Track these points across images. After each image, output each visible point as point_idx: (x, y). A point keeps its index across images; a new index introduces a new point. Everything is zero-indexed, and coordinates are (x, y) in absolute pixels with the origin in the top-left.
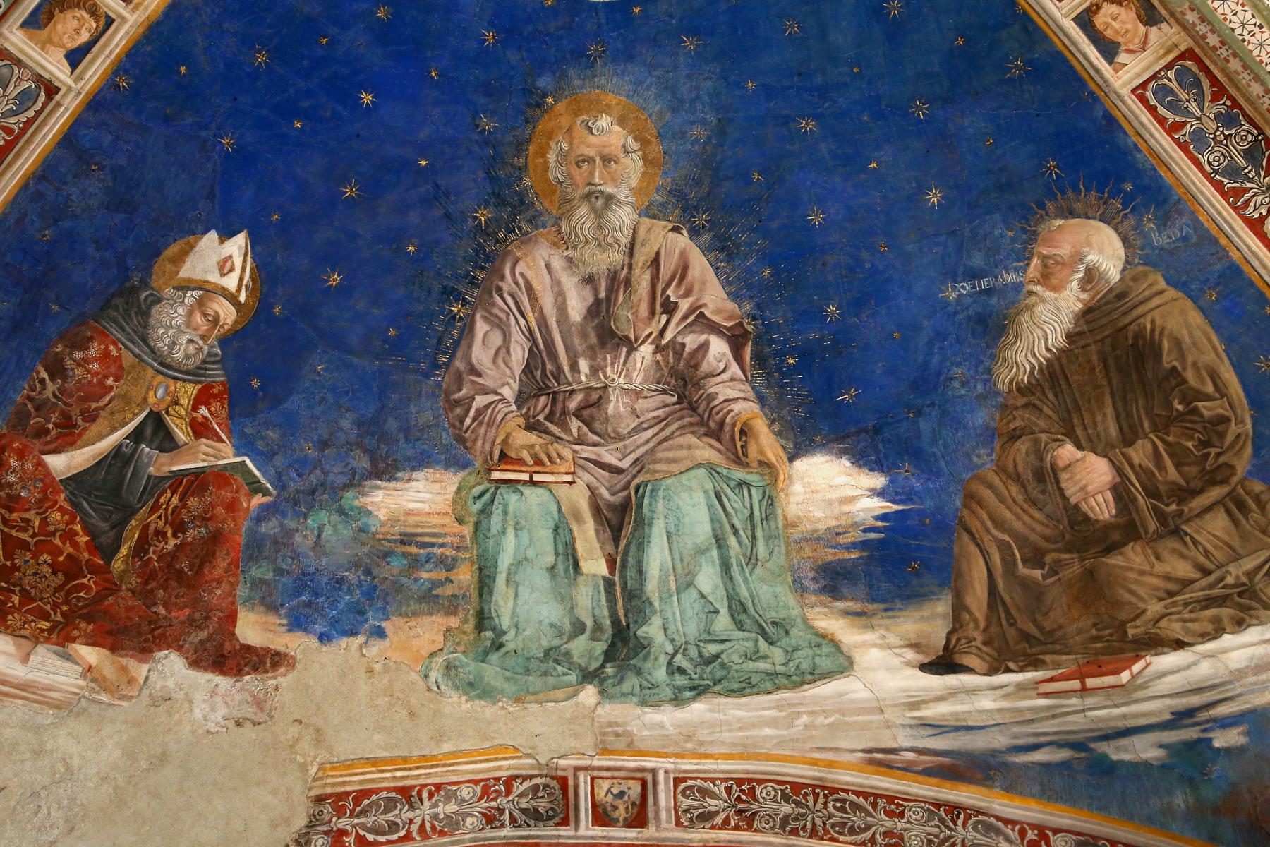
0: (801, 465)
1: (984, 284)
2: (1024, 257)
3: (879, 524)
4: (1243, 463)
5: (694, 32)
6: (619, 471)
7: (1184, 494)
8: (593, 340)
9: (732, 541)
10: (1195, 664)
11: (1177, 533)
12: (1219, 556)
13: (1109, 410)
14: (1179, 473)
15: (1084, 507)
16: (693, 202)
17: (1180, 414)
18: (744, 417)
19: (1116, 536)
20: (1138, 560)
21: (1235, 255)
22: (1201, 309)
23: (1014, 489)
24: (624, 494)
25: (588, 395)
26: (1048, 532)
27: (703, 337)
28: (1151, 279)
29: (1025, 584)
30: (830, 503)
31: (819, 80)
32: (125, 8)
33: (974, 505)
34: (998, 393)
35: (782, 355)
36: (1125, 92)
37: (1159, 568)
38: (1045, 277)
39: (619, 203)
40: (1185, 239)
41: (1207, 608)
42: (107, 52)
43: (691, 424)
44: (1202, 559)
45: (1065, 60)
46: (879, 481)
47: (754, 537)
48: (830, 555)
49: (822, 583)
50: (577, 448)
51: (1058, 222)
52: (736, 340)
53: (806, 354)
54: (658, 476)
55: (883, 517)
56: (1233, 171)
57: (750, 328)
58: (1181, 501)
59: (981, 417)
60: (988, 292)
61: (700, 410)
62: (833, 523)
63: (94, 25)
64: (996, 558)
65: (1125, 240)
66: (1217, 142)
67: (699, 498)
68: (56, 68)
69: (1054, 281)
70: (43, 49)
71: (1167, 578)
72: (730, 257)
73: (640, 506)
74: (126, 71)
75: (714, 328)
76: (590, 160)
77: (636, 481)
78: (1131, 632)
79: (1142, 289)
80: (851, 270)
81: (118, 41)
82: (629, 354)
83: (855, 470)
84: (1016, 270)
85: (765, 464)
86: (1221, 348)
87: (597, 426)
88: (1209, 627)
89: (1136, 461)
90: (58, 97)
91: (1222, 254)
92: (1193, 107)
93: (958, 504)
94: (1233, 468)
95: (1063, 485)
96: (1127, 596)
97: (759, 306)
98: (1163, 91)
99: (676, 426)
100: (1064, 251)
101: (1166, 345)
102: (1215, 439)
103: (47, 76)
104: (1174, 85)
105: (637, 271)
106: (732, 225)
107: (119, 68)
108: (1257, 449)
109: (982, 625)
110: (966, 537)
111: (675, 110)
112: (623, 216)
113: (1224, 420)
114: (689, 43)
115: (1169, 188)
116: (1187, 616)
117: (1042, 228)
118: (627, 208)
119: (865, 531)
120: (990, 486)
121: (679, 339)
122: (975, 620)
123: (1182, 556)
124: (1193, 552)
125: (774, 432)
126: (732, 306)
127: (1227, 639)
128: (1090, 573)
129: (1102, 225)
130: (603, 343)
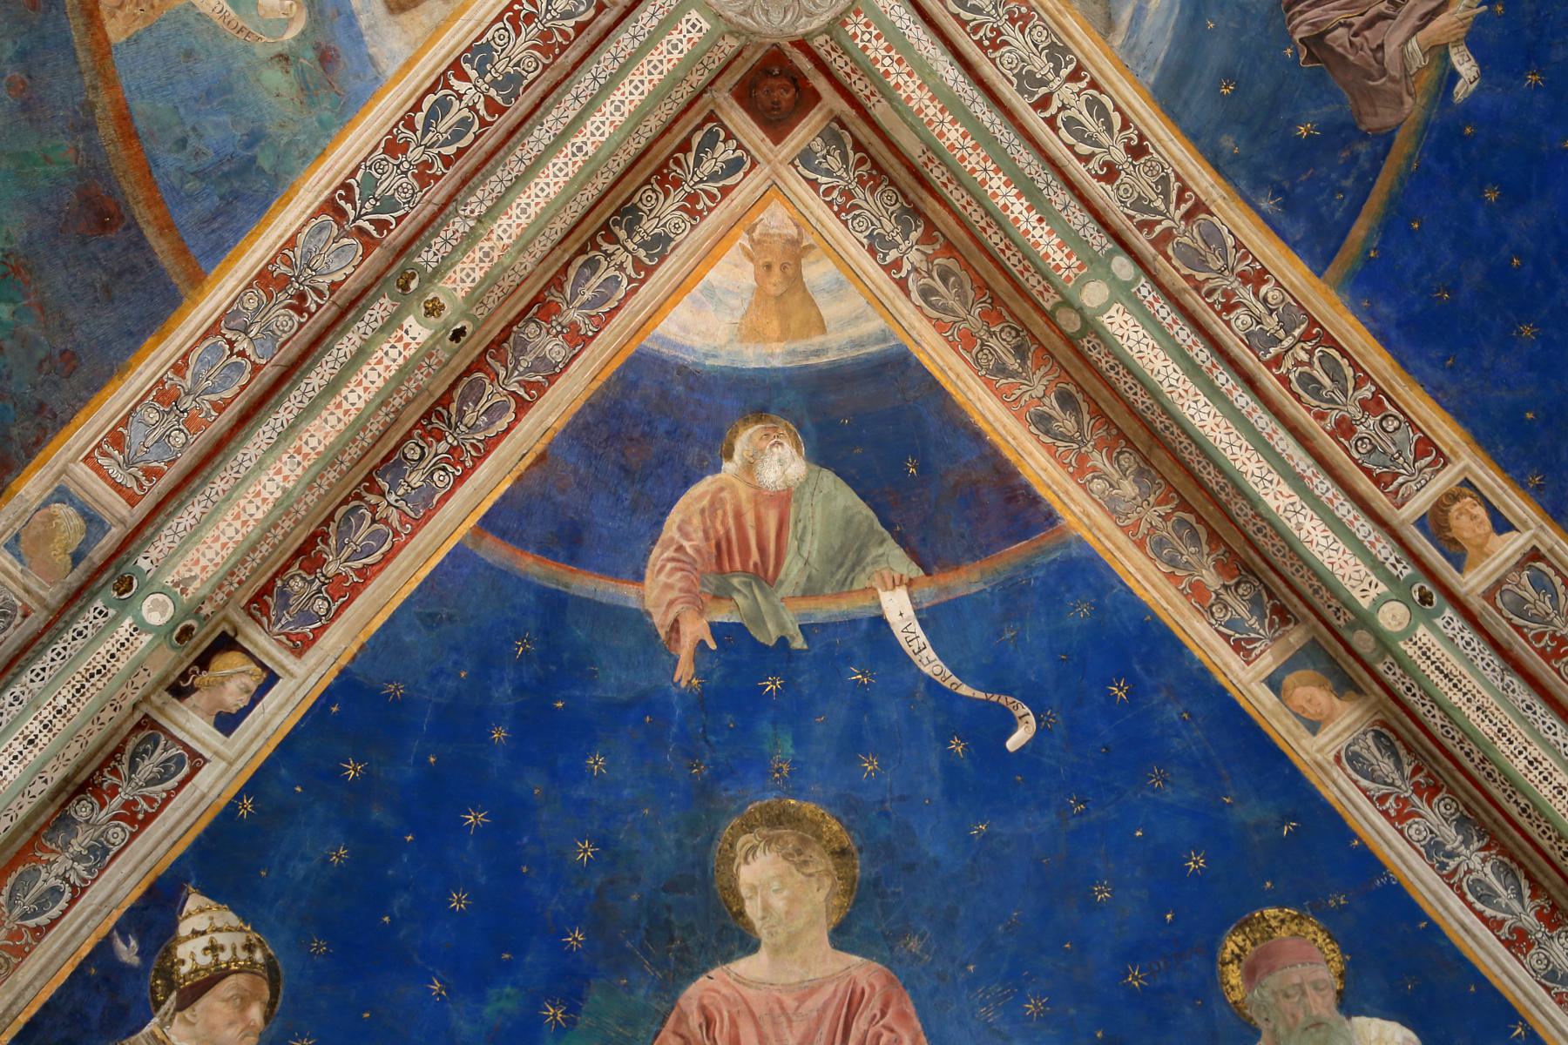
32: (1454, 465)
42: (1500, 491)
63: (1469, 499)
68: (1510, 547)
70: (1488, 556)
74: (1523, 475)
81: (1489, 478)
90: (1543, 550)
103: (1518, 557)
107: (1520, 483)
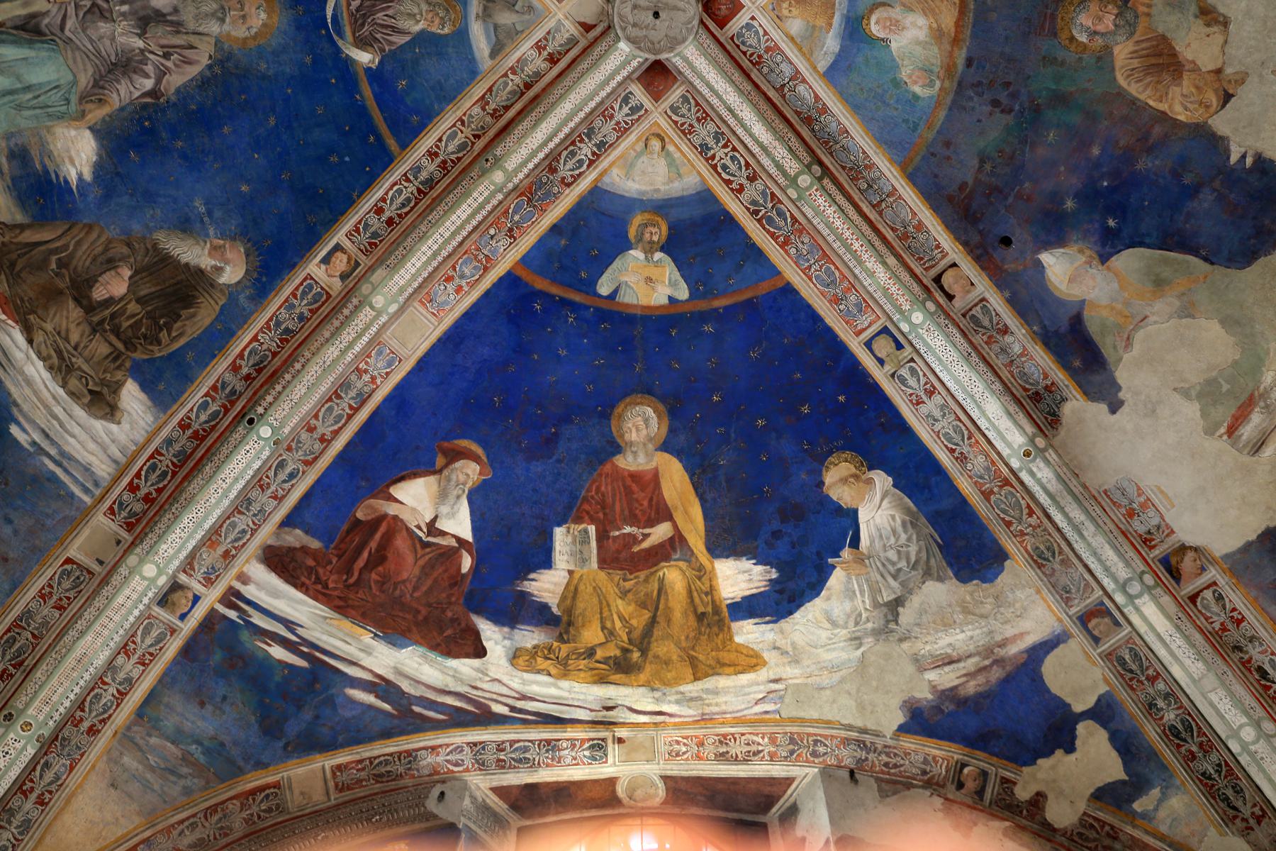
0: (88, 134)
1: (206, 219)
2: (223, 236)
3: (62, 179)
4: (138, 356)
5: (314, 62)
6: (62, 28)
7: (116, 332)
8: (142, 13)
9: (29, 96)
10: (20, 350)
11: (94, 331)
12: (86, 353)
13: (153, 289)
14: (127, 328)
15: (97, 285)
16: (226, 65)
17: (158, 322)
18: (109, 100)
19: (85, 302)
20: (75, 315)
21: (240, 333)
22: (212, 324)
23: (100, 249)
24: (47, 32)
25: (107, 11)
26: (79, 269)
27: (152, 75)
28: (223, 298)
29: (46, 261)
30: (68, 151)
31: (295, 125)
33: (86, 230)
34: (151, 234)
35: (149, 119)
36: (308, 271)
37: (72, 326)
38: (215, 248)
39: (221, 25)
40: (244, 309)
41: (55, 351)
43: (100, 71)
44: (82, 345)
45: (318, 241)
46: (88, 176)
47: (35, 108)
48: (34, 152)
49: (16, 149)
50: (73, 4)
51: (242, 250)
52: (154, 93)
53: (151, 132)
54: (63, 52)
55: (66, 181)
56: (278, 324)
57: (162, 100)
58: (112, 331)
59: (136, 227)
60: (202, 221)
61: (109, 75)
62: (56, 154)
64: (58, 244)
65: (239, 282)
66: (290, 315)
67: (54, 76)
69: (213, 252)
71: (68, 330)
72: (199, 87)
73: (43, 42)
75: (159, 81)
76: (242, 9)
77: (58, 40)
78: (31, 317)
79: (217, 294)
80: (203, 151)
82: (137, 34)
83: (91, 164)
84: (216, 233)
85: (83, 114)
86: (195, 335)
87: (89, 16)
88: (44, 354)
89: (129, 306)
91: (240, 327)
92: (305, 302)
93: (85, 221)
94: (135, 351)
95: (108, 273)
96: (52, 312)
97: (175, 104)
98: (310, 287)
99: (97, 62)
100: (229, 255)
101: (192, 310)
102: (149, 341)
104: (314, 291)
105: (185, 37)
106: (216, 87)
108: (147, 360)
109: (14, 240)
110: (66, 227)
111: (273, 53)
112: (214, 28)
113: (159, 343)
114: (308, 60)
115: (267, 297)
116: (48, 343)
117: (239, 243)
118: (219, 30)
119: (55, 172)
120: (99, 237)
121: (149, 62)
122: (16, 237)
123: (82, 336)
124: (85, 341)
125: (104, 118)
126: (172, 90)
127: (40, 364)
128: (61, 293)
129: (244, 271)
130: (140, 19)
